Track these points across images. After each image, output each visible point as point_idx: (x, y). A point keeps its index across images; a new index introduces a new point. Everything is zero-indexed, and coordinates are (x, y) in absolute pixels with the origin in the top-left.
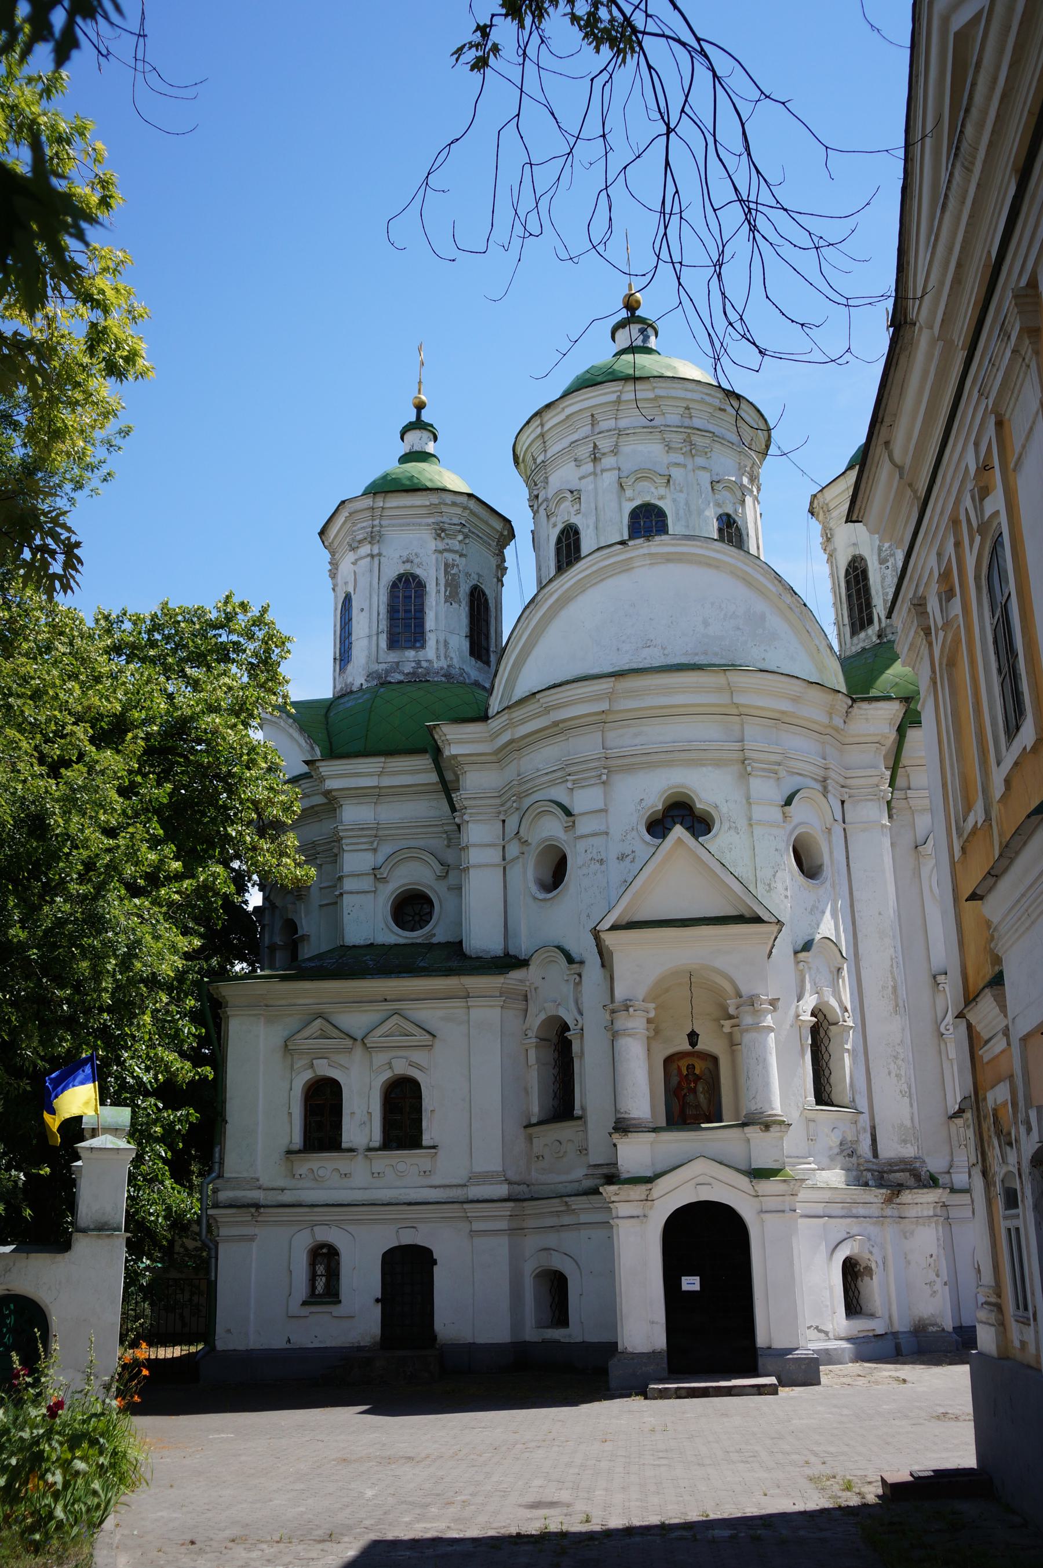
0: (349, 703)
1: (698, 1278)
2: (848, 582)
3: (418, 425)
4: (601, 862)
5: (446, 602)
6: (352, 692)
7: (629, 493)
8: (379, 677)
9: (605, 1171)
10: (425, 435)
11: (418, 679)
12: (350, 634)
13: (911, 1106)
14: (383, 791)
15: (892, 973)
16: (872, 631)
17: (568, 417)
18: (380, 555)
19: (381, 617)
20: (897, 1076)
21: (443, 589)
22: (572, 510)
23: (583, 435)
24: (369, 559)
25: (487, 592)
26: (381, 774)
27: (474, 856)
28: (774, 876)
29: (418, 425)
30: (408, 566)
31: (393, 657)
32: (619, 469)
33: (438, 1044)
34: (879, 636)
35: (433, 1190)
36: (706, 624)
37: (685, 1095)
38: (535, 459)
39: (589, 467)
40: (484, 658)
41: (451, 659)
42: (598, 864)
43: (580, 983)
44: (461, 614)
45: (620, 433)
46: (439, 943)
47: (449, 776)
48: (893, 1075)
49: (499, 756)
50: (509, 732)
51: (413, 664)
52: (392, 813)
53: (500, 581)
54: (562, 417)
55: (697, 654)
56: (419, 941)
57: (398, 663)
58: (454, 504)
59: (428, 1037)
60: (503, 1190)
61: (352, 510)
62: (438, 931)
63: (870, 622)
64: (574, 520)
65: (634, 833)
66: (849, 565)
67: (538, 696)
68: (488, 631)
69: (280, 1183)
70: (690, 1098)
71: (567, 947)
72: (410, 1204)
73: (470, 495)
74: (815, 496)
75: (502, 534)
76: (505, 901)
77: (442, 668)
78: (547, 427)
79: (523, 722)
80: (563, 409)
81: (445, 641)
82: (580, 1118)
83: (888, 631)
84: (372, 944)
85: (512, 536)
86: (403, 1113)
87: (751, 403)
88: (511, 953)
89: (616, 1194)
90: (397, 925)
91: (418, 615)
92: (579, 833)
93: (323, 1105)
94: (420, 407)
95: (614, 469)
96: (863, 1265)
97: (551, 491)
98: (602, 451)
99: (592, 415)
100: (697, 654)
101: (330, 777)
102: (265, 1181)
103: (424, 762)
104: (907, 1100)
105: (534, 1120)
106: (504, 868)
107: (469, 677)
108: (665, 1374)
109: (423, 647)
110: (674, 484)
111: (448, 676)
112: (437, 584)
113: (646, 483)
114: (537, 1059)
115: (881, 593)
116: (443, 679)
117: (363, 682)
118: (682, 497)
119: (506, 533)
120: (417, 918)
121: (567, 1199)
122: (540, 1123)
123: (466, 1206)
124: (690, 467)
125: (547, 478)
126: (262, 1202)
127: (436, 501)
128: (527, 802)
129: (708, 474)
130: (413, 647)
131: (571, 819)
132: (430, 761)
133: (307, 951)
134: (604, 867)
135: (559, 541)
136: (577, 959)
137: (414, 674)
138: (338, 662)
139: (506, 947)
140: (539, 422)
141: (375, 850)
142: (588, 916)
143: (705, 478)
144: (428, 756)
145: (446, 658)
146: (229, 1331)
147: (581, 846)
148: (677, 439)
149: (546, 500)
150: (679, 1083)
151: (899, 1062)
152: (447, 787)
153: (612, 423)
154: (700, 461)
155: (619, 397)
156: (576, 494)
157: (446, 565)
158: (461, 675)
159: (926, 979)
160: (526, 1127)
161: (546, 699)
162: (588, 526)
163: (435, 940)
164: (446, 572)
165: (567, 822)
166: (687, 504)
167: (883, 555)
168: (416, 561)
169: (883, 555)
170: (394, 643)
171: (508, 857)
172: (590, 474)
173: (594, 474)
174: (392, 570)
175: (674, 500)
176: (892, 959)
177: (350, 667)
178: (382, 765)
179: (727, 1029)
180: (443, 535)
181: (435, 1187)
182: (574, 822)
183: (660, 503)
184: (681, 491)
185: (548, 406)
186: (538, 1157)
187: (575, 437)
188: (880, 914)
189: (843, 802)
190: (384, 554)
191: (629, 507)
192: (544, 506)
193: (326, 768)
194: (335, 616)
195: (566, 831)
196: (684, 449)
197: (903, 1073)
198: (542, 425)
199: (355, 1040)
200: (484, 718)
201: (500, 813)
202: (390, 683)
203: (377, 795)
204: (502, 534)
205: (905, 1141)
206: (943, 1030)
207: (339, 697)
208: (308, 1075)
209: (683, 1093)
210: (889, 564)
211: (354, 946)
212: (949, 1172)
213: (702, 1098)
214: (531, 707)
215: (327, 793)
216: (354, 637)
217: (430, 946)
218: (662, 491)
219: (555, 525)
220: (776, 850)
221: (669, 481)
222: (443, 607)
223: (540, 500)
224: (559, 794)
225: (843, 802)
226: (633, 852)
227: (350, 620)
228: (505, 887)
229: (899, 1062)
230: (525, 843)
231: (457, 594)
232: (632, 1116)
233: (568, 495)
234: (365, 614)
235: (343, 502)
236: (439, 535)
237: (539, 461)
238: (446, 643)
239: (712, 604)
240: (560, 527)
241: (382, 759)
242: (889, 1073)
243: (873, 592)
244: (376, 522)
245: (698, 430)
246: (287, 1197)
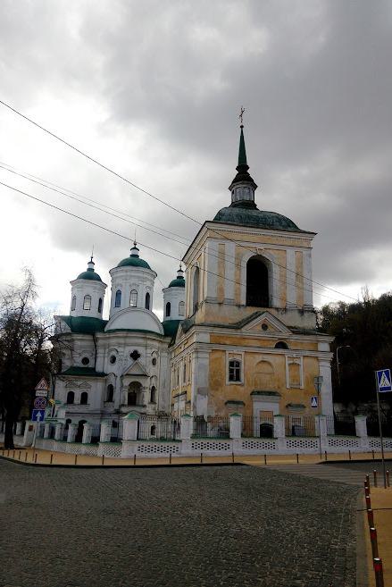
3: (91, 263)
29: (91, 263)
52: (84, 343)
62: (91, 365)
86: (84, 397)
93: (71, 396)
156: (122, 286)
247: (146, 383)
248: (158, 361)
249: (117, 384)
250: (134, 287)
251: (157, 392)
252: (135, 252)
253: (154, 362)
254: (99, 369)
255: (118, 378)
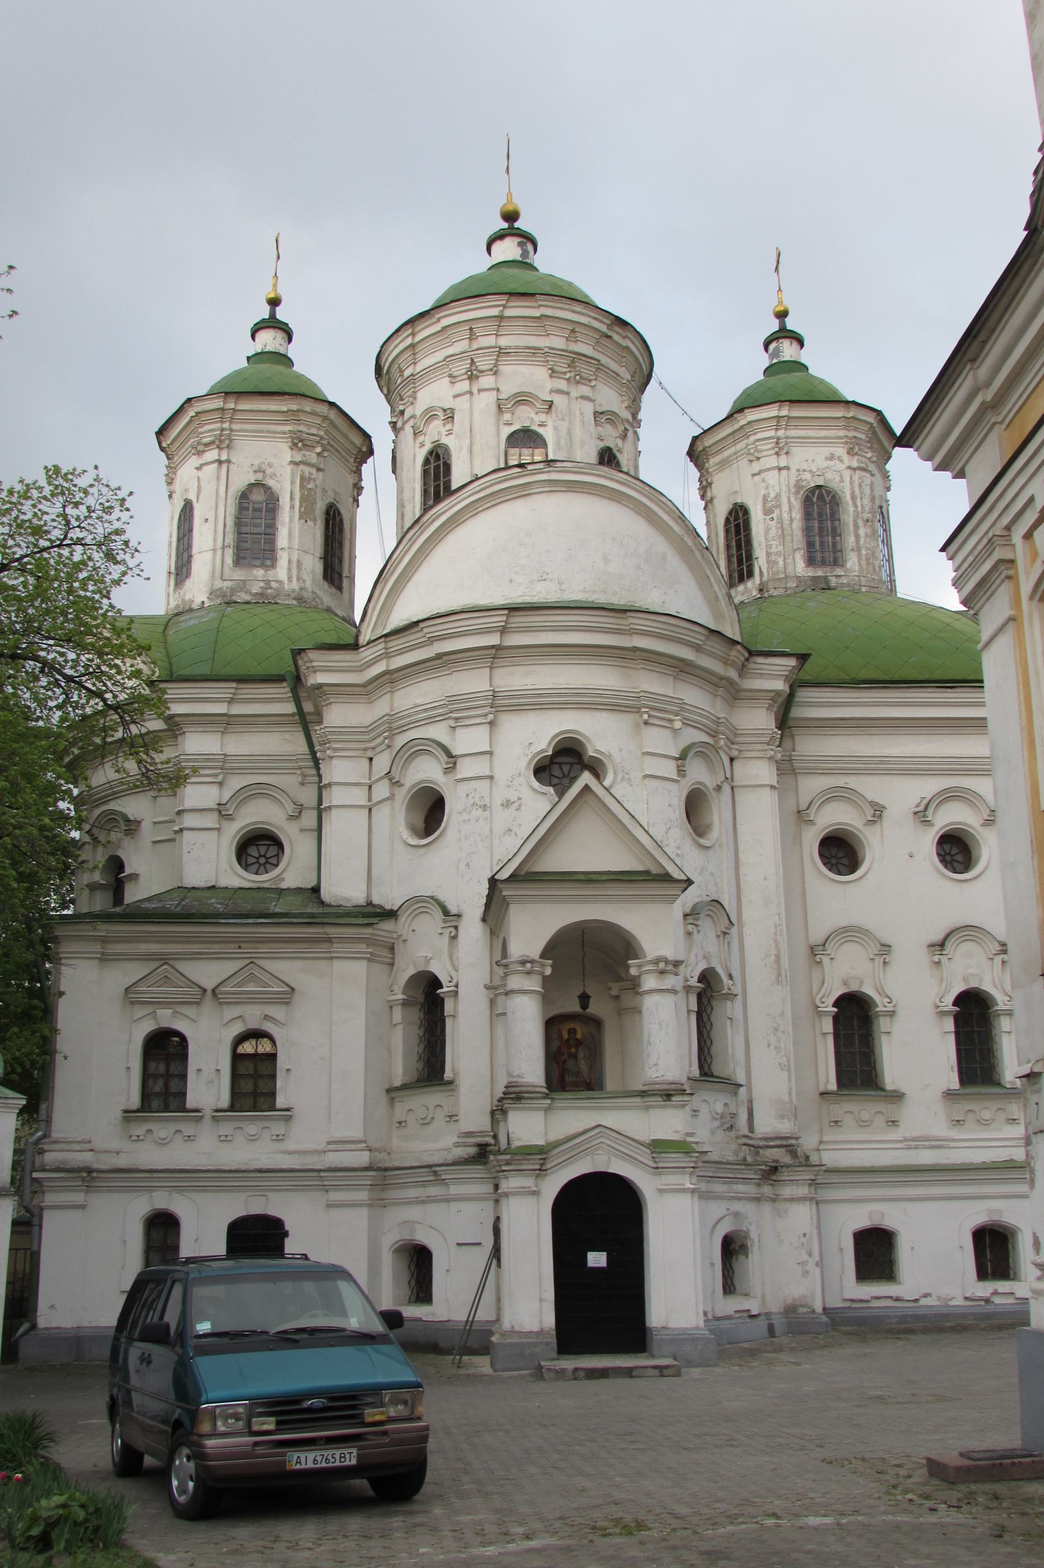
0: (189, 622)
1: (589, 1253)
2: (727, 531)
4: (484, 808)
5: (300, 518)
6: (191, 610)
7: (507, 417)
8: (224, 596)
9: (478, 1140)
10: (280, 335)
11: (266, 600)
12: (189, 547)
13: (790, 1080)
14: (232, 719)
15: (775, 941)
16: (751, 586)
17: (444, 329)
18: (228, 461)
19: (227, 529)
20: (776, 1048)
21: (297, 504)
22: (444, 431)
23: (457, 351)
24: (216, 465)
25: (343, 512)
26: (231, 701)
27: (335, 797)
28: (667, 833)
30: (260, 476)
31: (239, 574)
32: (498, 390)
33: (297, 997)
34: (761, 590)
35: (287, 1157)
36: (606, 560)
37: (565, 1061)
38: (402, 372)
39: (464, 386)
40: (336, 582)
41: (304, 581)
42: (480, 811)
43: (454, 938)
44: (316, 532)
45: (501, 352)
46: (288, 889)
47: (308, 707)
48: (772, 1047)
49: (369, 688)
50: (385, 661)
51: (262, 584)
52: (242, 745)
53: (356, 501)
54: (438, 327)
55: (595, 592)
56: (266, 885)
57: (244, 582)
58: (313, 413)
59: (286, 989)
60: (362, 1158)
61: (199, 409)
63: (750, 574)
64: (444, 440)
65: (521, 779)
66: (730, 513)
67: (421, 625)
68: (342, 554)
69: (115, 1144)
70: (570, 1064)
71: (442, 898)
72: (260, 1171)
73: (332, 404)
74: (695, 439)
75: (360, 451)
76: (370, 846)
77: (293, 591)
78: (418, 338)
79: (401, 652)
80: (439, 320)
81: (299, 561)
82: (450, 1083)
83: (771, 585)
84: (213, 887)
85: (371, 452)
87: (638, 333)
88: (376, 900)
89: (508, 1163)
90: (240, 864)
91: (269, 531)
92: (459, 777)
94: (274, 303)
95: (493, 389)
96: (739, 1243)
97: (419, 408)
98: (481, 368)
99: (471, 329)
100: (595, 592)
101: (174, 701)
102: (97, 1144)
103: (283, 690)
104: (786, 1074)
105: (397, 1083)
106: (370, 810)
107: (322, 602)
108: (555, 1354)
109: (273, 566)
110: (556, 411)
111: (300, 599)
112: (292, 499)
113: (525, 408)
114: (403, 1017)
115: (763, 545)
116: (295, 602)
117: (205, 599)
118: (564, 426)
119: (364, 449)
120: (262, 860)
121: (437, 1169)
122: (404, 1087)
123: (322, 1174)
124: (574, 394)
125: (415, 392)
126: (96, 1166)
127: (295, 407)
128: (401, 740)
129: (592, 404)
130: (262, 566)
131: (452, 760)
132: (288, 689)
133: (133, 894)
134: (487, 813)
135: (427, 461)
136: (453, 910)
137: (262, 595)
138: (173, 577)
139: (369, 895)
140: (410, 331)
141: (221, 784)
142: (468, 865)
143: (588, 408)
144: (285, 684)
145: (298, 579)
146: (52, 1307)
147: (463, 789)
148: (562, 366)
149: (413, 417)
150: (559, 1048)
151: (779, 1034)
152: (305, 722)
153: (491, 341)
154: (584, 390)
155: (502, 311)
156: (450, 416)
157: (302, 478)
158: (314, 599)
159: (803, 951)
160: (388, 1091)
161: (429, 630)
162: (461, 448)
163: (284, 885)
164: (302, 487)
165: (447, 763)
166: (570, 433)
167: (768, 505)
168: (269, 471)
169: (768, 505)
170: (239, 560)
171: (375, 799)
172: (466, 393)
173: (471, 393)
174: (242, 478)
175: (555, 428)
176: (776, 927)
177: (188, 583)
178: (233, 691)
179: (614, 992)
180: (300, 445)
181: (290, 1153)
182: (455, 763)
183: (540, 430)
184: (563, 419)
185: (423, 315)
186: (400, 1123)
187: (451, 351)
188: (765, 879)
189: (732, 760)
190: (233, 460)
191: (506, 431)
192: (411, 423)
193: (173, 691)
194: (172, 525)
195: (445, 773)
196: (568, 376)
197: (783, 1046)
198: (413, 334)
199: (205, 990)
200: (355, 646)
201: (365, 750)
202: (235, 602)
203: (227, 723)
204: (360, 451)
205: (782, 1117)
206: (818, 1003)
207: (177, 615)
208: (148, 1027)
209: (563, 1058)
210: (774, 515)
211: (194, 888)
212: (818, 1150)
213: (583, 1065)
214: (413, 638)
215: (170, 719)
216: (195, 550)
217: (281, 892)
218: (543, 417)
219: (422, 445)
220: (670, 805)
221: (550, 406)
222: (297, 524)
223: (407, 415)
224: (438, 732)
225: (732, 760)
226: (520, 799)
227: (191, 530)
228: (370, 830)
229: (779, 1034)
230: (396, 784)
231: (313, 511)
232: (525, 1080)
233: (440, 414)
234: (211, 524)
235: (189, 400)
236: (295, 445)
237: (407, 373)
238: (299, 564)
239: (614, 539)
240: (428, 446)
241: (234, 685)
242: (769, 1045)
243: (755, 543)
244: (226, 425)
245: (584, 355)
246: (122, 1162)
247: (655, 930)
248: (718, 814)
249: (464, 966)
250: (526, 417)
251: (733, 1009)
252: (508, 250)
253: (695, 806)
254: (344, 886)
255: (472, 929)
